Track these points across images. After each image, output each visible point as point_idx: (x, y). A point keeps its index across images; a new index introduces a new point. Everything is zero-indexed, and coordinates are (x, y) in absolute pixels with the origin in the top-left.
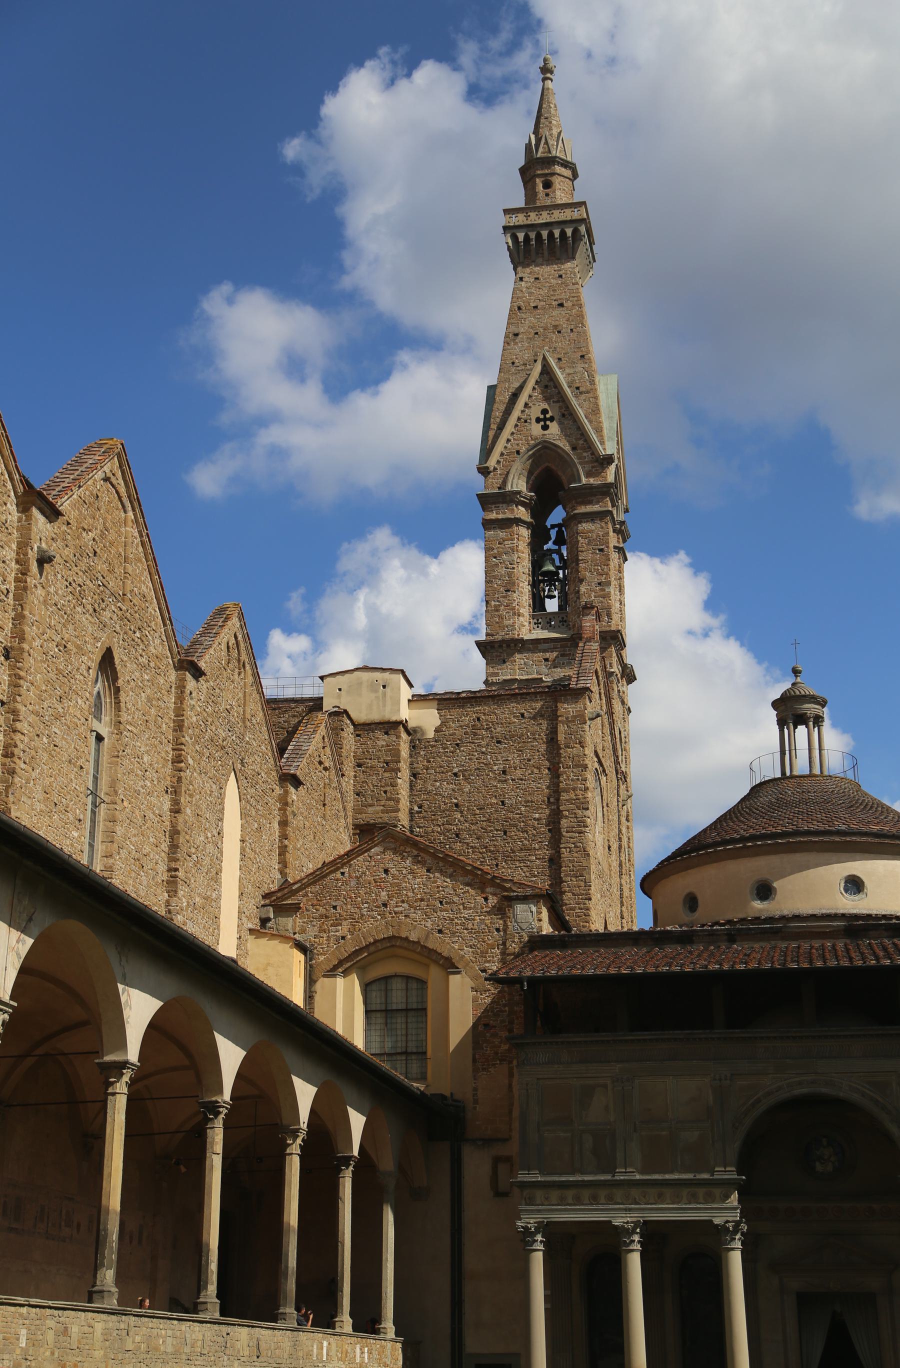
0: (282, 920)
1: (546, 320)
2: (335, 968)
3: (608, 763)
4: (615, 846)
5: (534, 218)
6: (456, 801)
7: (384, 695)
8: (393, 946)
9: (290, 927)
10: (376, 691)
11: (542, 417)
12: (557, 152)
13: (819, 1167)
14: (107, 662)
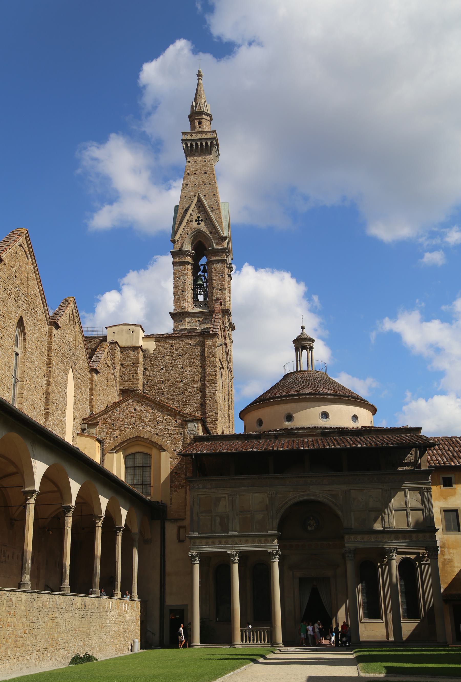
0: (91, 430)
1: (200, 179)
2: (113, 449)
3: (225, 364)
4: (227, 398)
5: (194, 137)
6: (162, 380)
7: (133, 335)
8: (137, 440)
9: (94, 432)
10: (129, 334)
11: (198, 219)
12: (204, 110)
13: (309, 528)
14: (21, 323)
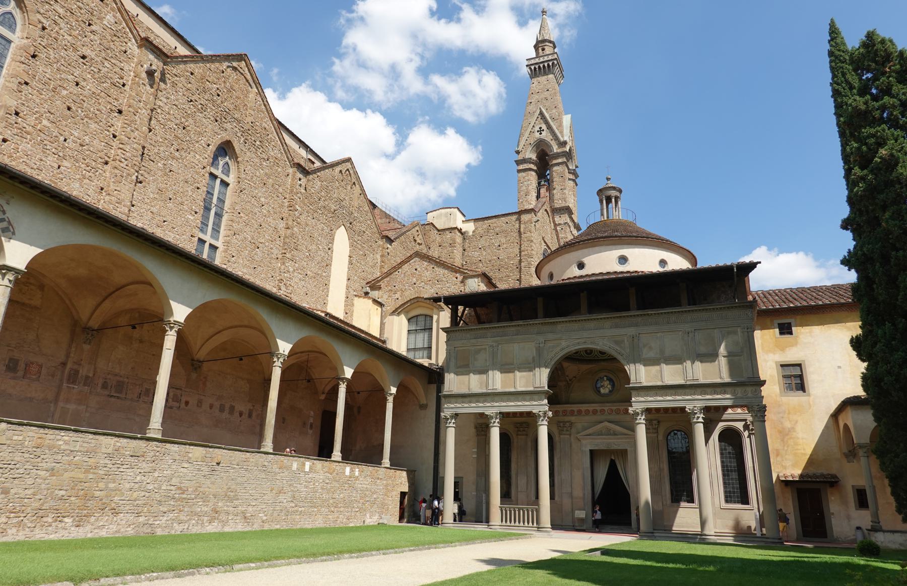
1: (543, 96)
2: (394, 312)
7: (450, 218)
8: (417, 301)
13: (602, 391)
